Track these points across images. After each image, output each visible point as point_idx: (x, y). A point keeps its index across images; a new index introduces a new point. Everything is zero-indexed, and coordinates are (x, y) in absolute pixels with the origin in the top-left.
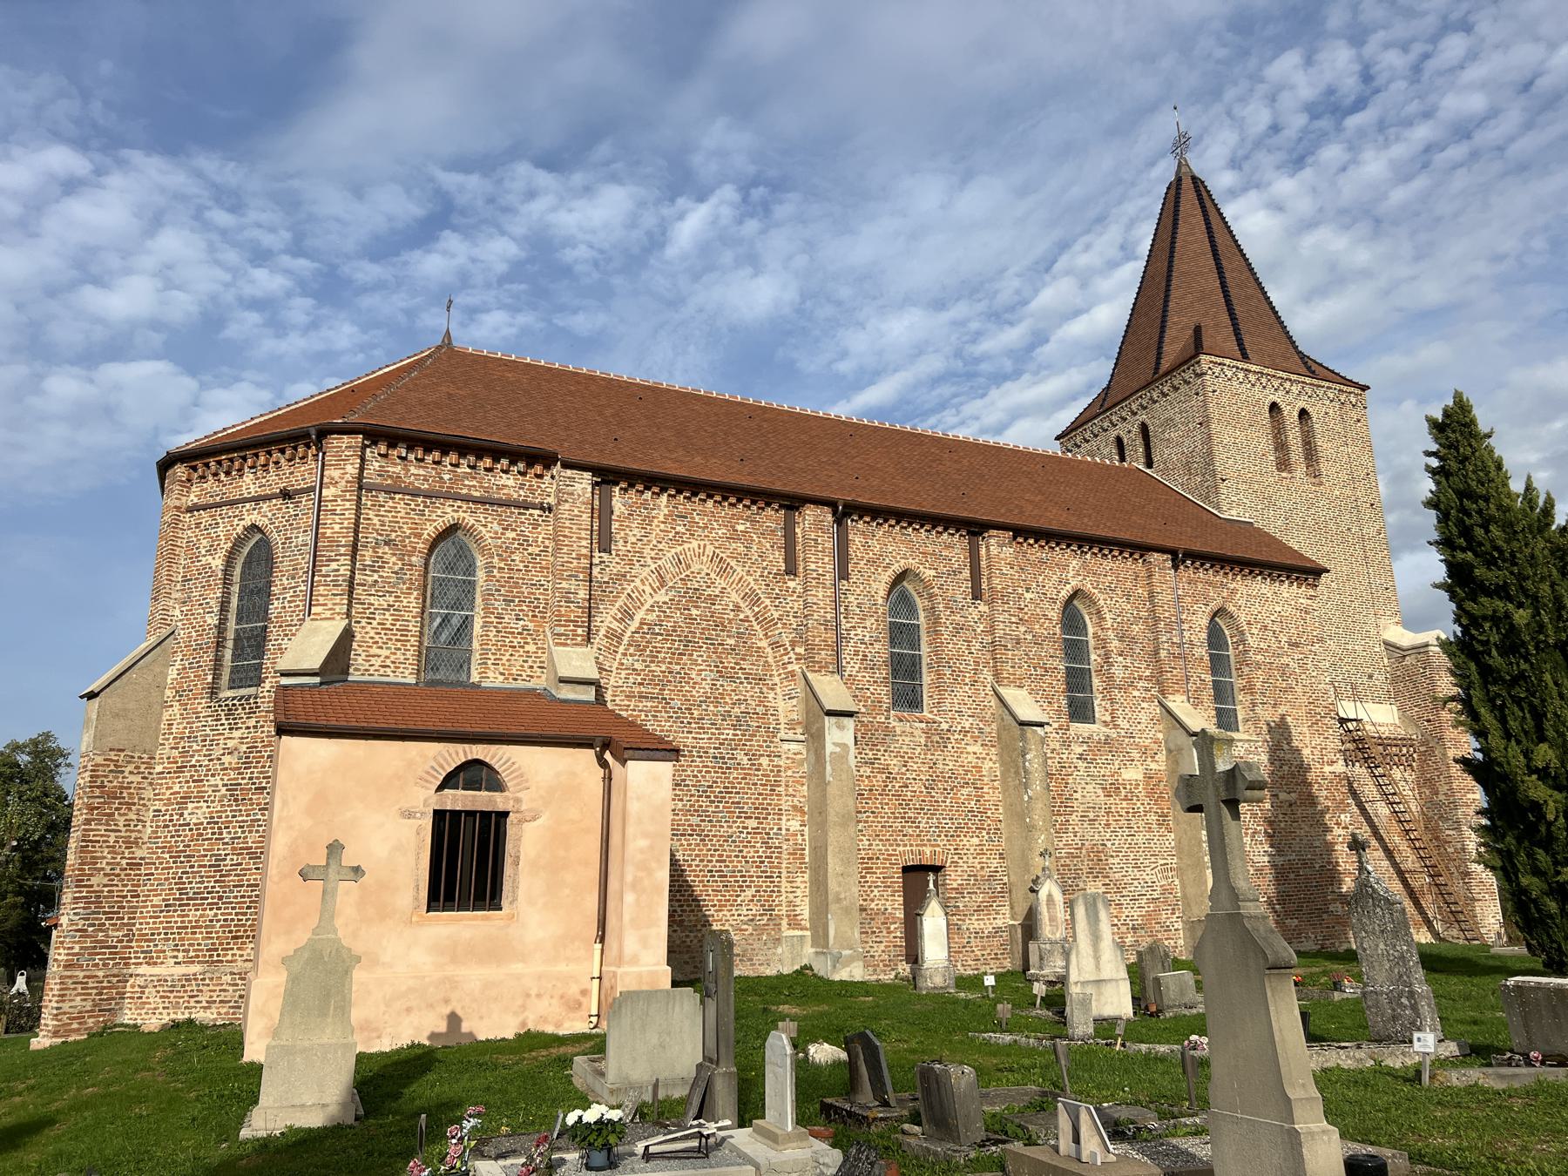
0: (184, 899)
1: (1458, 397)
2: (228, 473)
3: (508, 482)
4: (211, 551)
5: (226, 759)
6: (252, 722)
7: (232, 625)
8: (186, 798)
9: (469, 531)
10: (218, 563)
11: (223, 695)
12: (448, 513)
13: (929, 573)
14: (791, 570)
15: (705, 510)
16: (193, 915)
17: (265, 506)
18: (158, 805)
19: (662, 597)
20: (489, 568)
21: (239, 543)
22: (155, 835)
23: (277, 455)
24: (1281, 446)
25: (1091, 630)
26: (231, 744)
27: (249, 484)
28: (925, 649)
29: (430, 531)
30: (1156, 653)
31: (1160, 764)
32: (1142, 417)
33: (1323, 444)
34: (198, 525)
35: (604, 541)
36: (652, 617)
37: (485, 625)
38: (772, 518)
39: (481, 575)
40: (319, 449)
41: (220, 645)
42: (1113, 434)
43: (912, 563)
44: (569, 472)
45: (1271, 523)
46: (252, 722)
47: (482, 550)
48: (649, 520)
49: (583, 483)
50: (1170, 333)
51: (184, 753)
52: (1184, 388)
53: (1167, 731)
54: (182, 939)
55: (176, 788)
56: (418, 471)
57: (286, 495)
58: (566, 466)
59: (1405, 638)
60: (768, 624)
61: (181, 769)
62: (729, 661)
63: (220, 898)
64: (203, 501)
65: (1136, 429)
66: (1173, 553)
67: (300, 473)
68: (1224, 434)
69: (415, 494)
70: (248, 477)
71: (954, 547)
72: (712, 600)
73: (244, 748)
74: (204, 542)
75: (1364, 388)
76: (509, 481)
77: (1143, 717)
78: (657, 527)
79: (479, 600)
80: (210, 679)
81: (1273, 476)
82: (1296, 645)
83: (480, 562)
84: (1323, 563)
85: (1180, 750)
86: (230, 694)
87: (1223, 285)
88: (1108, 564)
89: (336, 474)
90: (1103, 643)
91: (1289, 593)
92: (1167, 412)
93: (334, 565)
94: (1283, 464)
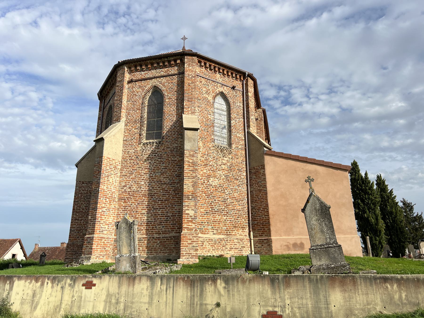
0: (213, 212)
1: (354, 161)
4: (207, 93)
5: (223, 166)
6: (230, 157)
8: (209, 176)
16: (218, 217)
17: (225, 88)
26: (224, 161)
27: (218, 76)
34: (201, 82)
46: (230, 157)
51: (206, 160)
54: (215, 225)
55: (205, 171)
61: (206, 165)
63: (227, 213)
73: (229, 164)
74: (204, 89)
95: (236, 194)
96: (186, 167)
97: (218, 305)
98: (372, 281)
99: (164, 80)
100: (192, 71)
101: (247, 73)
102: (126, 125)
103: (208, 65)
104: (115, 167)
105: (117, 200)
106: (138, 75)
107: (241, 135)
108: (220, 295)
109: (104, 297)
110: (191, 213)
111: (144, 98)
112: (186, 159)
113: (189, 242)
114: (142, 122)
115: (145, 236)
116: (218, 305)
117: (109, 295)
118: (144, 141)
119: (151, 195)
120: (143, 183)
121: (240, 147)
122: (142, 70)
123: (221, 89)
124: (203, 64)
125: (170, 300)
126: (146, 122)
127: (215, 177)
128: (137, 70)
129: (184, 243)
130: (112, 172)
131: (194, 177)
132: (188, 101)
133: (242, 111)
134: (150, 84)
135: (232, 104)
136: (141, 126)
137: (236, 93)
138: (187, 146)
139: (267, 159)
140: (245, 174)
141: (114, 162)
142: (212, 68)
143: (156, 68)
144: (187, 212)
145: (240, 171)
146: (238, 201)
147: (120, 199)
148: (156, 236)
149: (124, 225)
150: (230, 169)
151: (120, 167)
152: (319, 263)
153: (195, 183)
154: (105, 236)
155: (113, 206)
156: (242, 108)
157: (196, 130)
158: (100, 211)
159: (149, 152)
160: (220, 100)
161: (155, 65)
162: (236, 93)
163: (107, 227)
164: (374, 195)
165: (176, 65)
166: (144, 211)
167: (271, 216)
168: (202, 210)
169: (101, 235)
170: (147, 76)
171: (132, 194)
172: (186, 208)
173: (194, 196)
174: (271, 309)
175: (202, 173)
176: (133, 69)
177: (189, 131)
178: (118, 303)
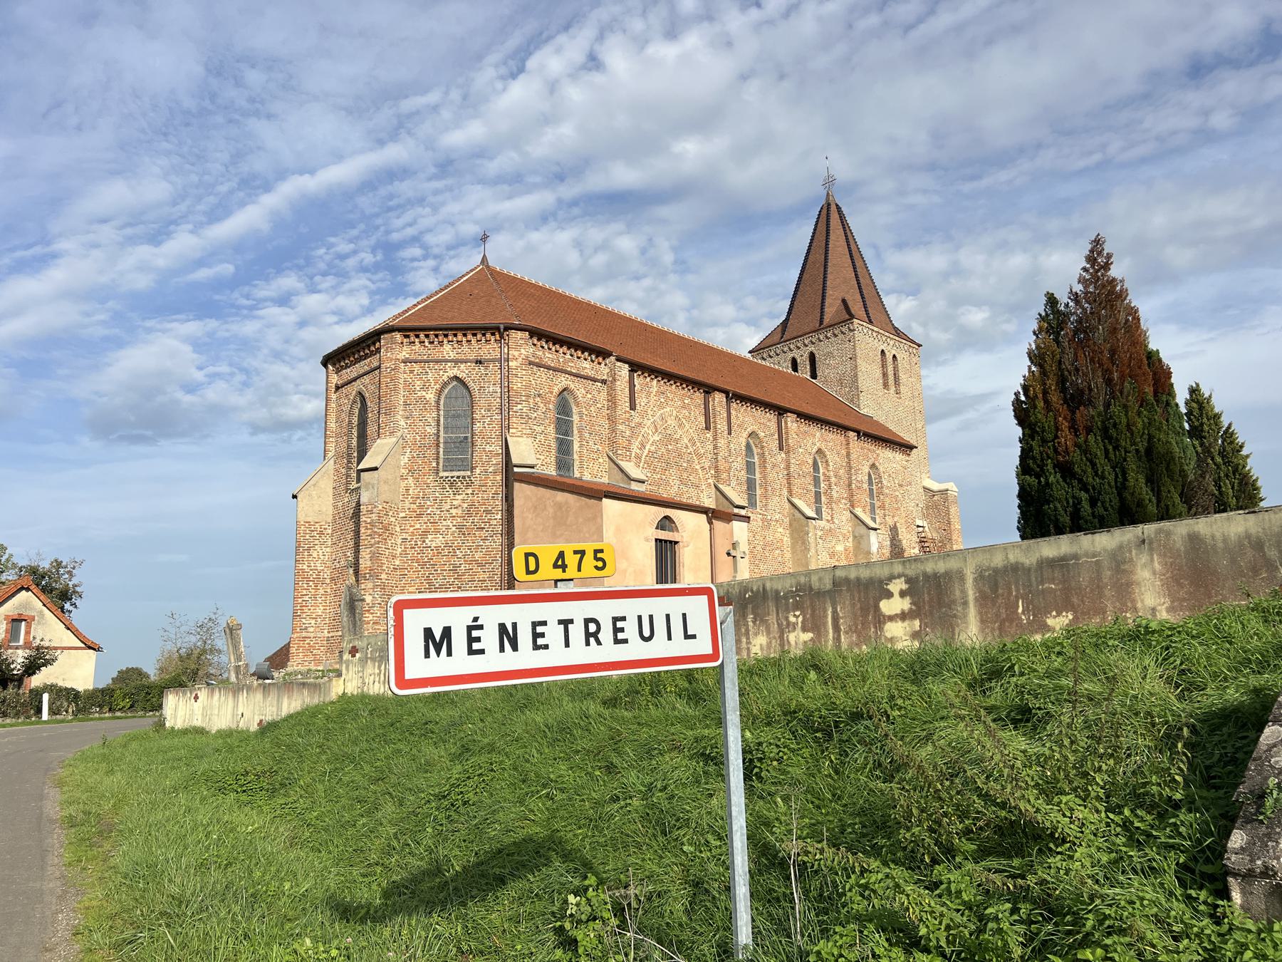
3: (586, 365)
5: (454, 511)
6: (470, 491)
7: (442, 433)
8: (426, 533)
9: (571, 392)
10: (431, 396)
11: (441, 474)
12: (563, 381)
14: (708, 428)
15: (673, 390)
17: (462, 366)
18: (404, 536)
19: (657, 438)
20: (580, 413)
21: (445, 385)
22: (404, 553)
23: (470, 337)
24: (885, 375)
25: (821, 471)
26: (455, 503)
27: (448, 350)
28: (758, 476)
29: (556, 390)
30: (850, 485)
31: (850, 544)
32: (811, 348)
33: (902, 376)
34: (412, 372)
35: (633, 407)
36: (653, 448)
37: (581, 446)
38: (699, 396)
39: (575, 418)
40: (502, 337)
41: (438, 445)
42: (790, 355)
43: (755, 428)
44: (619, 364)
45: (880, 417)
46: (470, 491)
47: (578, 405)
48: (649, 393)
49: (624, 370)
51: (421, 506)
52: (841, 336)
53: (854, 526)
55: (418, 526)
56: (550, 355)
57: (479, 362)
59: (935, 486)
60: (700, 456)
61: (420, 515)
62: (685, 475)
64: (413, 357)
65: (806, 355)
66: (858, 432)
67: (489, 348)
68: (862, 365)
69: (549, 368)
70: (447, 347)
71: (770, 418)
72: (677, 441)
75: (919, 346)
76: (587, 364)
77: (844, 518)
78: (653, 398)
79: (575, 432)
80: (434, 464)
82: (901, 486)
84: (913, 442)
85: (861, 537)
86: (446, 474)
87: (856, 276)
88: (831, 436)
89: (516, 353)
90: (828, 478)
92: (828, 348)
93: (520, 407)
94: (886, 385)
99: (366, 379)
103: (422, 336)
104: (321, 533)
105: (328, 581)
123: (451, 373)
127: (437, 532)
128: (342, 368)
134: (353, 390)
135: (476, 393)
136: (349, 462)
140: (499, 516)
142: (432, 337)
145: (487, 512)
146: (480, 565)
147: (332, 579)
155: (322, 591)
157: (376, 469)
163: (313, 622)
169: (304, 634)
170: (354, 375)
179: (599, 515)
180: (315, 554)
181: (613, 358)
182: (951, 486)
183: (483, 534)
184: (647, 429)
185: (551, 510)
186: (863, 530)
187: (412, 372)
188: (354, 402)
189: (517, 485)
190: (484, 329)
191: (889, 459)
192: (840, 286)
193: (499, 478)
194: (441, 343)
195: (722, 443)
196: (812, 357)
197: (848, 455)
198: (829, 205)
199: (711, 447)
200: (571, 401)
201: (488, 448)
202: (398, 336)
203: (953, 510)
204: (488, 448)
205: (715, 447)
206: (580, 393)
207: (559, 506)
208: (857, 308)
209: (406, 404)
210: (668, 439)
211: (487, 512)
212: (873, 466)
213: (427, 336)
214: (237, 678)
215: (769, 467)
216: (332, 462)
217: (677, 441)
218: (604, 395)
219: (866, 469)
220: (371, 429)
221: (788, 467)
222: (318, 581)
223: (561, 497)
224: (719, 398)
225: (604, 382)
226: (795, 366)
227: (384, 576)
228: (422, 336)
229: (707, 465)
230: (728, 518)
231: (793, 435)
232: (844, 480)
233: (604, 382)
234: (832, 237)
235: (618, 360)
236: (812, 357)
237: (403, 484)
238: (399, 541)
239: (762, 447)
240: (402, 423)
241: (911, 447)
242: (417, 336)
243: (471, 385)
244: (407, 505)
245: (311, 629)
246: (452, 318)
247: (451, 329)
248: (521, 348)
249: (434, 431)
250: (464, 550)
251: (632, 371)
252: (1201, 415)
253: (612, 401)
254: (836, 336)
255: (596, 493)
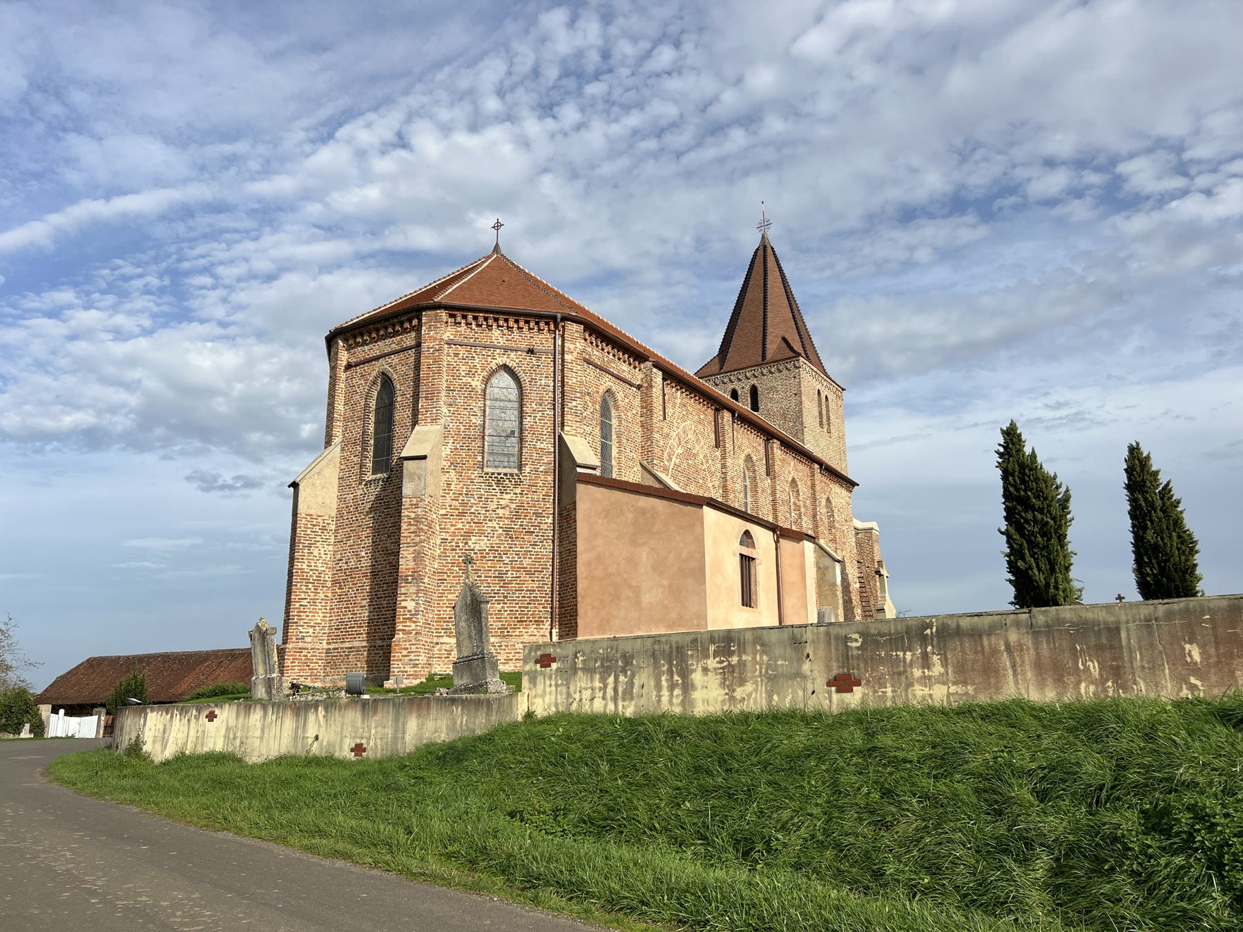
1: (1012, 423)
2: (479, 326)
4: (471, 373)
6: (518, 491)
8: (468, 534)
10: (477, 383)
11: (486, 470)
12: (608, 382)
13: (755, 458)
17: (512, 355)
18: (444, 535)
20: (619, 417)
22: (444, 555)
26: (502, 502)
27: (496, 335)
28: (749, 499)
29: (602, 389)
30: (814, 516)
32: (754, 381)
33: (832, 417)
34: (456, 355)
40: (556, 327)
42: (731, 387)
44: (655, 370)
46: (518, 491)
47: (617, 408)
49: (658, 376)
50: (769, 338)
51: (463, 504)
52: (785, 372)
55: (460, 526)
57: (531, 351)
58: (656, 366)
60: (712, 474)
61: (462, 514)
65: (748, 388)
67: (542, 339)
69: (596, 366)
72: (695, 455)
73: (514, 506)
74: (464, 368)
76: (625, 367)
79: (614, 437)
80: (480, 458)
81: (818, 429)
83: (614, 413)
85: (826, 568)
88: (801, 466)
89: (572, 347)
90: (798, 508)
91: (844, 492)
93: (574, 403)
94: (821, 424)
95: (526, 562)
96: (404, 526)
97: (317, 738)
98: (442, 701)
99: (395, 359)
100: (435, 339)
101: (559, 316)
102: (343, 449)
103: (470, 317)
104: (324, 529)
105: (329, 584)
106: (363, 352)
107: (548, 445)
108: (320, 726)
109: (223, 732)
110: (410, 605)
111: (368, 396)
112: (405, 513)
113: (405, 652)
114: (364, 443)
115: (365, 644)
116: (317, 738)
117: (228, 729)
118: (369, 476)
119: (374, 575)
120: (363, 554)
121: (542, 469)
122: (365, 343)
123: (501, 360)
124: (459, 319)
125: (278, 734)
126: (372, 442)
127: (481, 533)
128: (357, 344)
129: (396, 655)
130: (318, 538)
131: (416, 544)
132: (427, 398)
133: (551, 394)
134: (374, 370)
135: (526, 385)
136: (364, 449)
137: (539, 359)
138: (408, 489)
139: (581, 488)
140: (550, 520)
141: (320, 520)
143: (384, 338)
144: (403, 604)
145: (537, 515)
146: (529, 573)
147: (335, 582)
148: (379, 643)
149: (257, 635)
150: (517, 514)
151: (333, 527)
152: (461, 682)
153: (419, 553)
154: (309, 646)
155: (322, 596)
156: (551, 389)
157: (424, 457)
158: (297, 605)
159: (373, 498)
160: (504, 380)
161: (381, 333)
162: (539, 359)
163: (311, 630)
164: (1049, 511)
165: (413, 328)
166: (364, 603)
167: (579, 599)
168: (450, 597)
169: (301, 645)
171: (351, 573)
172: (403, 597)
173: (417, 577)
174: (358, 741)
175: (452, 529)
176: (351, 342)
177: (410, 462)
178: (234, 738)
179: (701, 520)
180: (316, 552)
181: (649, 364)
182: (874, 525)
183: (532, 538)
184: (673, 442)
185: (630, 516)
186: (828, 561)
187: (456, 355)
188: (374, 383)
189: (581, 488)
190: (539, 317)
191: (838, 493)
192: (779, 327)
193: (550, 478)
194: (489, 327)
195: (729, 462)
196: (754, 391)
197: (813, 486)
198: (765, 247)
199: (719, 466)
200: (611, 403)
201: (539, 445)
202: (443, 314)
203: (876, 548)
204: (539, 445)
205: (724, 466)
206: (620, 396)
207: (643, 512)
208: (797, 347)
209: (448, 389)
210: (689, 454)
211: (537, 515)
212: (828, 500)
213: (475, 318)
214: (269, 692)
215: (760, 490)
216: (338, 449)
217: (695, 455)
218: (637, 402)
219: (824, 503)
220: (402, 414)
221: (774, 493)
222: (319, 583)
223: (644, 502)
224: (727, 415)
225: (639, 387)
226: (734, 394)
227: (426, 580)
228: (470, 317)
229: (717, 484)
230: (798, 537)
231: (778, 462)
232: (810, 512)
233: (639, 387)
234: (770, 278)
235: (655, 366)
236: (754, 391)
237: (444, 478)
238: (438, 542)
239: (754, 471)
240: (444, 410)
241: (854, 484)
242: (464, 317)
243: (521, 375)
244: (448, 501)
245: (309, 639)
246: (500, 302)
247: (503, 313)
248: (576, 342)
249: (479, 422)
250: (512, 555)
251: (664, 379)
252: (1142, 470)
253: (647, 407)
254: (780, 371)
255: (697, 502)
